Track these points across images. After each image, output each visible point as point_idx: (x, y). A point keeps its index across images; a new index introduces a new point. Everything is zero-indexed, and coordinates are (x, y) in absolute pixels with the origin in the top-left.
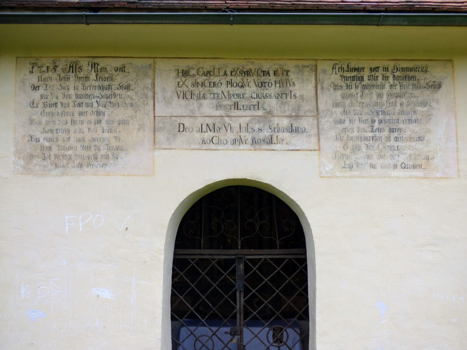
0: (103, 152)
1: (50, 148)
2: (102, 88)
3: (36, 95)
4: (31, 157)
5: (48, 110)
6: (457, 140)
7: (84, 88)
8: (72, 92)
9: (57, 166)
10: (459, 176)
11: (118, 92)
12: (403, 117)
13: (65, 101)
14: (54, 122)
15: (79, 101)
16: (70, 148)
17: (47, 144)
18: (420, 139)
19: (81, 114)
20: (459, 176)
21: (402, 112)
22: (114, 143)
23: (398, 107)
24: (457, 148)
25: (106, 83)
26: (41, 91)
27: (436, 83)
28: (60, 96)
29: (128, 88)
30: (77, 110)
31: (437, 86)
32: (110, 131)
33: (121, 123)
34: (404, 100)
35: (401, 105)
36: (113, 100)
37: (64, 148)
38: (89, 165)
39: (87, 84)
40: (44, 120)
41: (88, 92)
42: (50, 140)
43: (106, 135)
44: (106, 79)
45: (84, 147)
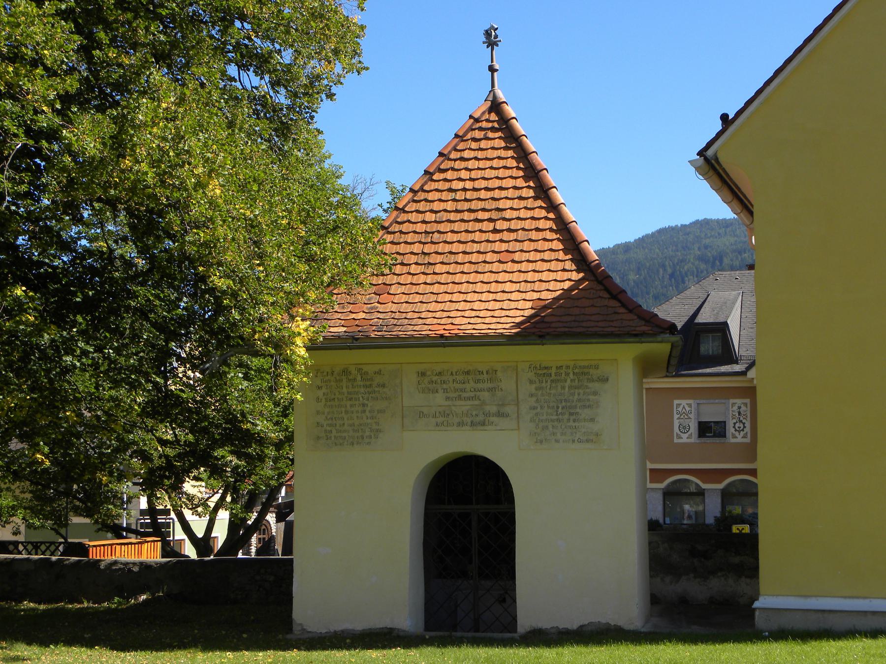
0: (367, 433)
1: (331, 431)
2: (366, 386)
3: (320, 393)
4: (318, 438)
5: (329, 403)
7: (353, 387)
8: (345, 390)
9: (336, 444)
11: (376, 389)
12: (579, 404)
13: (340, 397)
14: (333, 413)
15: (350, 396)
16: (345, 431)
17: (329, 428)
18: (592, 420)
19: (351, 406)
21: (579, 400)
22: (375, 427)
23: (576, 397)
25: (368, 383)
26: (324, 390)
28: (337, 394)
29: (383, 386)
30: (349, 403)
32: (372, 418)
33: (379, 411)
34: (581, 391)
35: (579, 394)
36: (373, 395)
37: (340, 431)
38: (358, 443)
39: (355, 384)
40: (327, 410)
41: (356, 390)
42: (330, 425)
43: (369, 421)
44: (368, 380)
45: (354, 431)
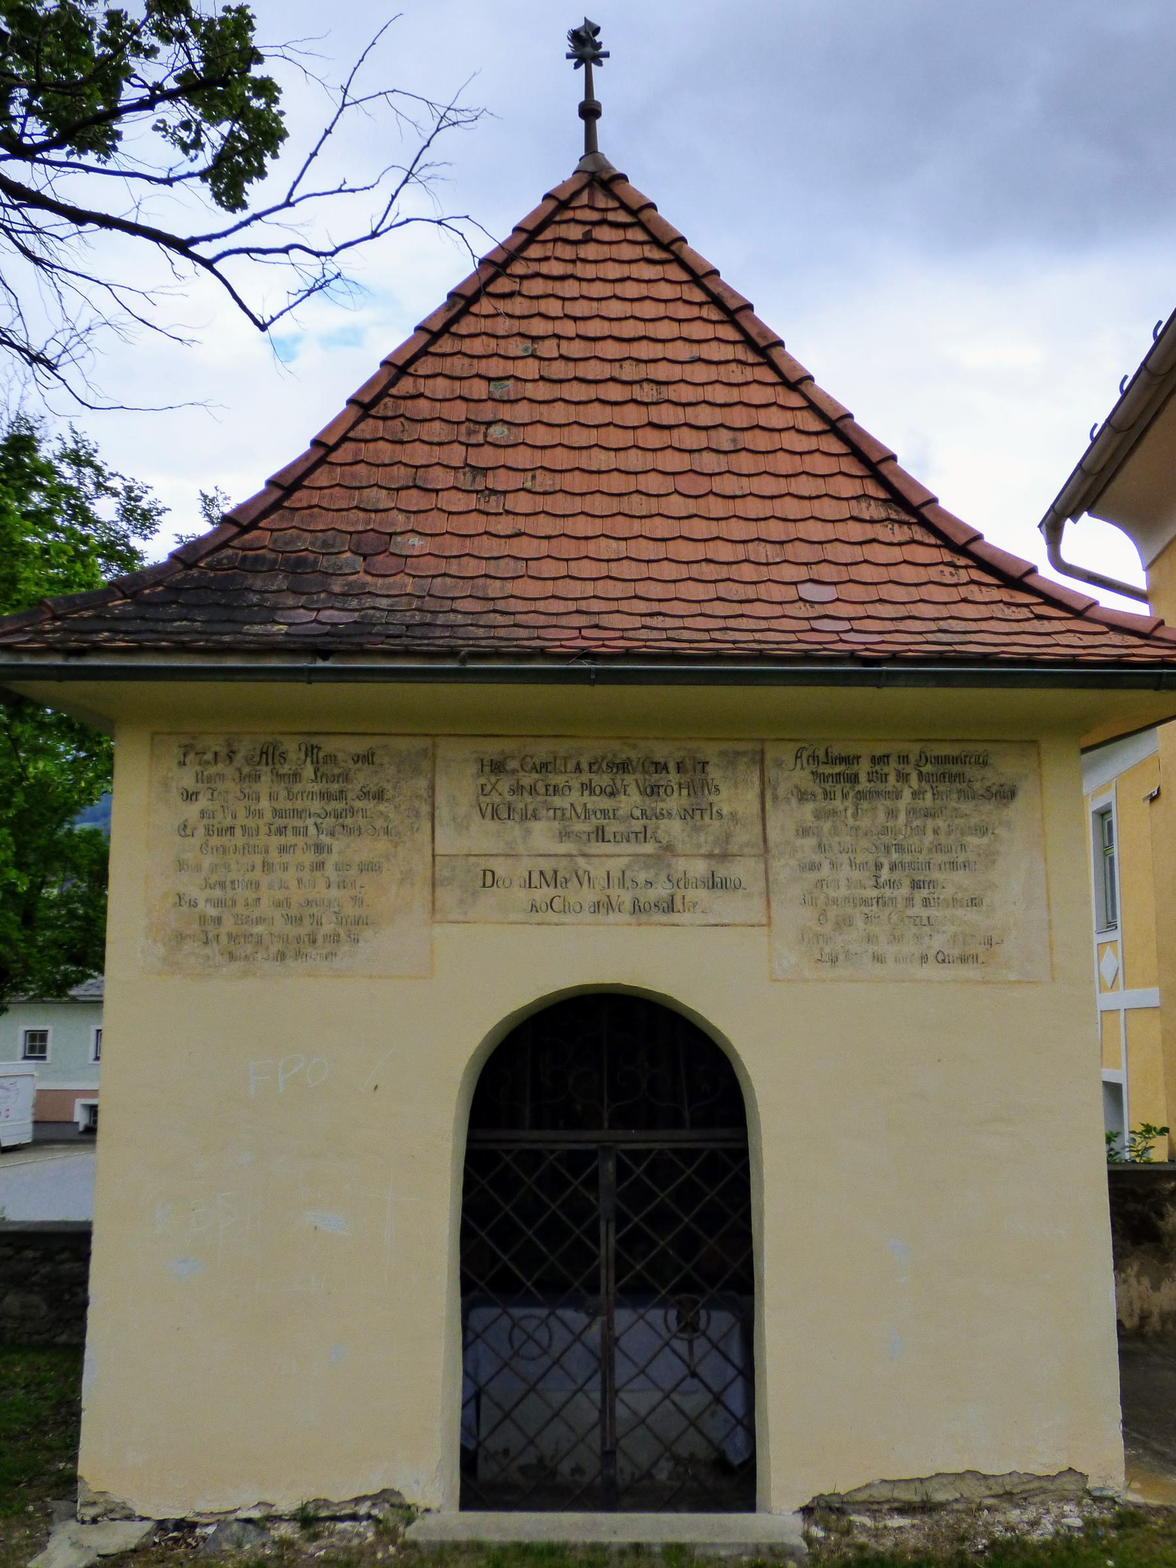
0: (328, 928)
1: (219, 920)
2: (325, 796)
3: (192, 811)
4: (180, 937)
5: (215, 841)
6: (1049, 905)
7: (291, 797)
8: (265, 804)
9: (232, 957)
10: (1053, 979)
11: (358, 804)
12: (939, 858)
13: (251, 823)
14: (227, 866)
15: (280, 822)
16: (260, 920)
17: (212, 912)
18: (974, 902)
19: (283, 849)
20: (1053, 979)
21: (938, 848)
22: (350, 911)
23: (929, 837)
24: (1050, 921)
25: (335, 787)
26: (203, 803)
27: (1006, 788)
28: (242, 813)
29: (379, 796)
30: (275, 841)
31: (1006, 794)
32: (342, 885)
33: (368, 867)
34: (941, 823)
35: (936, 832)
36: (349, 821)
37: (247, 920)
38: (298, 954)
39: (297, 788)
40: (207, 861)
41: (299, 804)
42: (219, 903)
43: (334, 893)
44: (335, 778)
45: (289, 919)
